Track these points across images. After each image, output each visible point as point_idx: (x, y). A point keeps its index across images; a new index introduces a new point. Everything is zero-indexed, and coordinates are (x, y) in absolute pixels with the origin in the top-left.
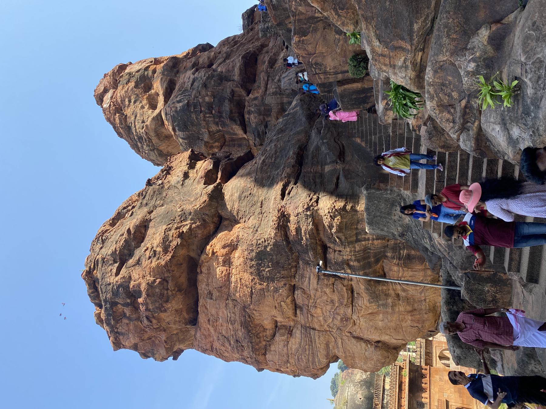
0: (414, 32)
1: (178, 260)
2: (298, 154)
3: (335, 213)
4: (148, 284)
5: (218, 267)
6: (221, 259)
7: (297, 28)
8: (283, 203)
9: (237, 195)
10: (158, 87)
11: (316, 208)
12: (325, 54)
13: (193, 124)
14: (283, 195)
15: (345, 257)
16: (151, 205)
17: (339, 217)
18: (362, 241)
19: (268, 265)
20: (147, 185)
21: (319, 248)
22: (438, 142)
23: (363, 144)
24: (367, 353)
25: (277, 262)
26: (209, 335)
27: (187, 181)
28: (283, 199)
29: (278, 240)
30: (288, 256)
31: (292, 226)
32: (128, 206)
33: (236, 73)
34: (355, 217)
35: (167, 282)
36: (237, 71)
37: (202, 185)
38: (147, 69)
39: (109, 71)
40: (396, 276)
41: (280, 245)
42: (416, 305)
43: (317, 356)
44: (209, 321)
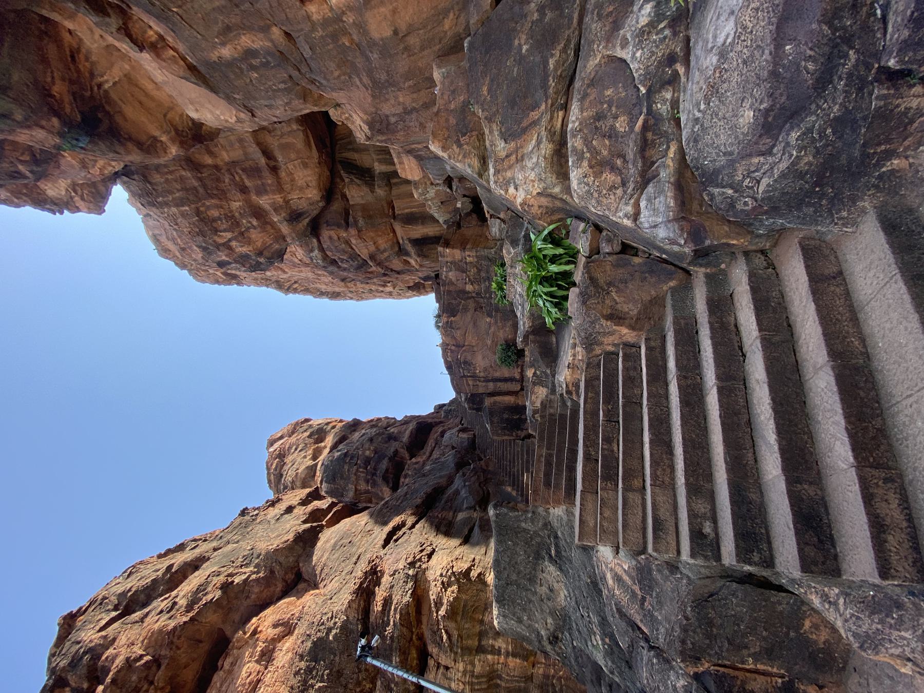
0: (549, 76)
1: (199, 630)
4: (128, 659)
5: (249, 662)
6: (261, 646)
8: (382, 552)
10: (329, 440)
11: (424, 566)
12: (475, 349)
13: (342, 478)
14: (387, 542)
17: (455, 588)
21: (414, 654)
23: (514, 493)
27: (286, 516)
28: (384, 547)
29: (351, 618)
35: (159, 666)
36: (408, 433)
38: (327, 424)
39: (294, 421)
41: (352, 631)
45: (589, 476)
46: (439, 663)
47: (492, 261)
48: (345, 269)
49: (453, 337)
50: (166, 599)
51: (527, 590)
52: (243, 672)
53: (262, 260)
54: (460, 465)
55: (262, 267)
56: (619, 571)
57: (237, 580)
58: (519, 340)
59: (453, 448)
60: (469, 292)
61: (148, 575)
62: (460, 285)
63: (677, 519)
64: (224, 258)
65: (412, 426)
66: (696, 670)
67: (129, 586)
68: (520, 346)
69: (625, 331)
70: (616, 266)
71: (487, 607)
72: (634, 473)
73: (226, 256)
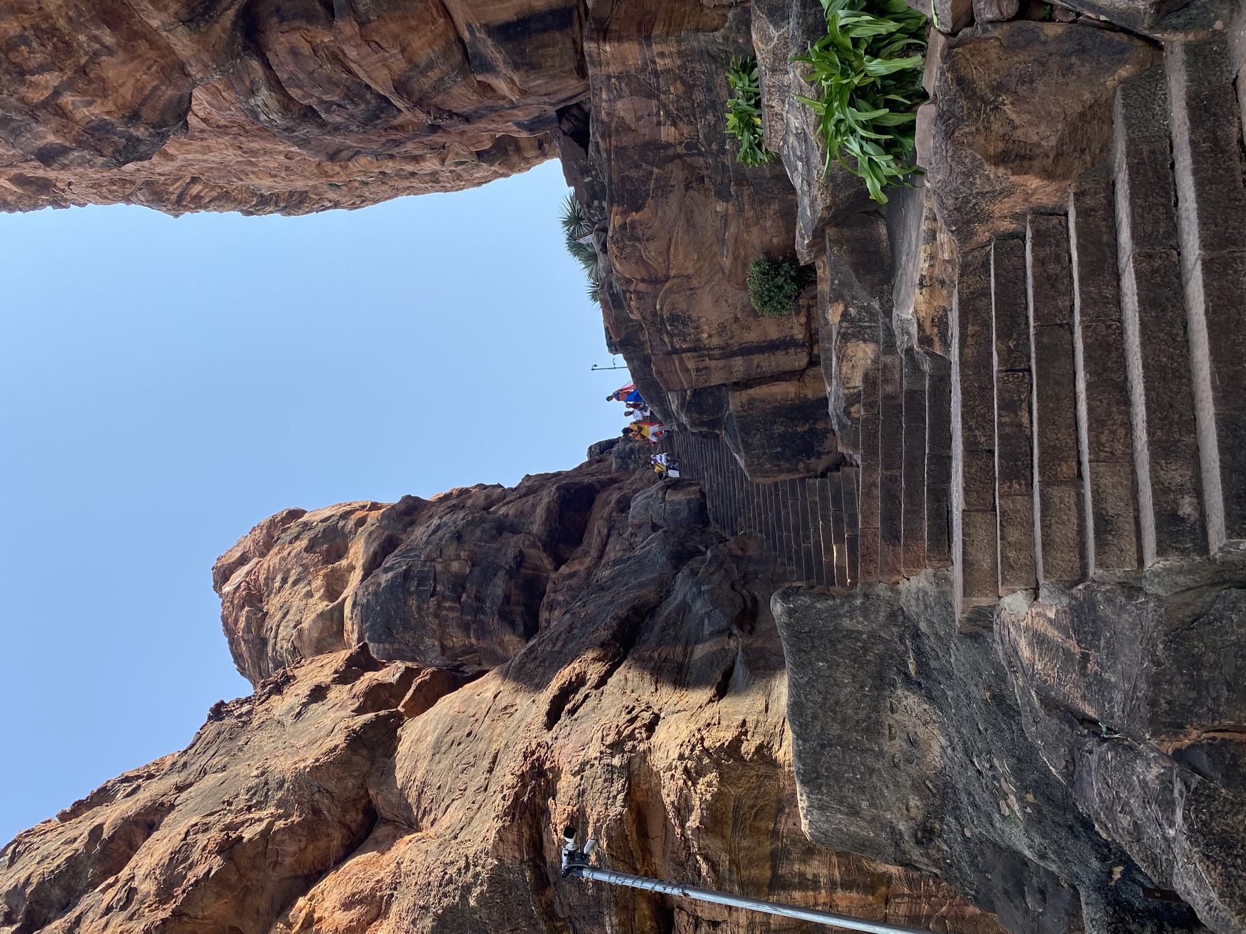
2: (627, 618)
3: (700, 759)
7: (615, 179)
8: (547, 737)
10: (358, 552)
11: (642, 747)
12: (695, 283)
13: (406, 626)
14: (553, 717)
16: (194, 767)
17: (712, 776)
18: (795, 888)
20: (210, 718)
27: (314, 706)
28: (549, 726)
29: (508, 861)
31: (560, 808)
36: (540, 512)
38: (345, 515)
39: (264, 519)
41: (513, 886)
45: (977, 485)
46: (697, 918)
47: (717, 59)
48: (336, 129)
49: (641, 261)
50: (110, 886)
51: (864, 751)
53: (140, 132)
54: (681, 557)
55: (142, 148)
56: (1041, 626)
58: (802, 243)
59: (655, 527)
60: (668, 145)
61: (55, 850)
62: (646, 131)
63: (1137, 510)
64: (51, 138)
65: (547, 496)
66: (1177, 745)
67: (23, 876)
68: (804, 258)
69: (1033, 182)
70: (1009, 47)
71: (785, 804)
72: (1060, 453)
73: (56, 132)
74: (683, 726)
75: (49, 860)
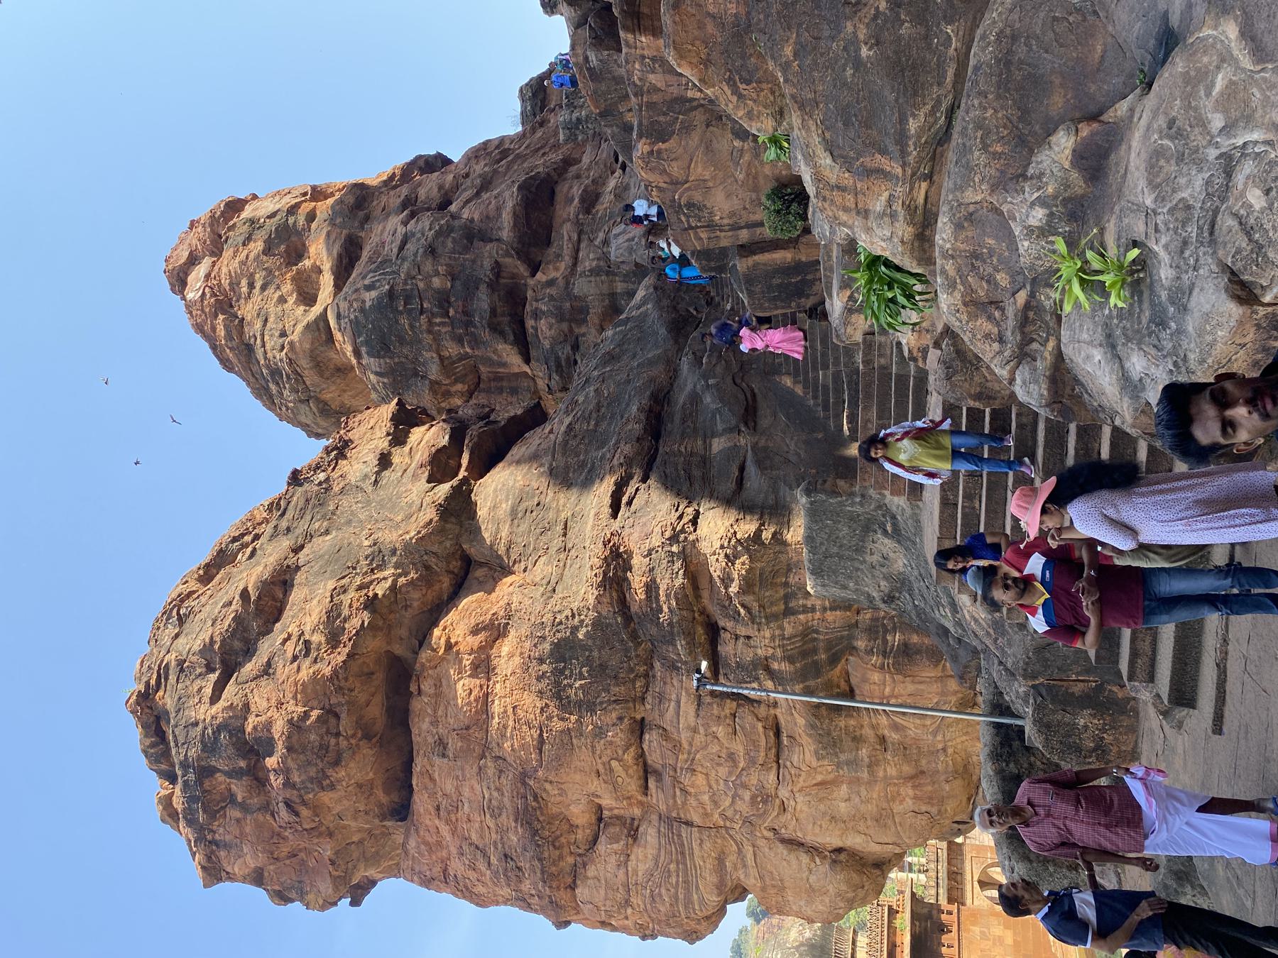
0: (908, 138)
2: (650, 411)
3: (735, 547)
4: (290, 722)
5: (459, 679)
6: (467, 661)
8: (615, 525)
9: (506, 507)
10: (320, 253)
11: (691, 538)
12: (711, 184)
13: (402, 341)
14: (615, 508)
15: (759, 652)
16: (298, 531)
19: (581, 673)
20: (289, 484)
21: (700, 630)
22: (966, 385)
23: (799, 390)
24: (813, 878)
25: (601, 665)
26: (439, 844)
27: (386, 473)
29: (604, 613)
30: (627, 650)
31: (637, 579)
32: (243, 535)
33: (506, 224)
34: (783, 557)
35: (337, 716)
36: (506, 218)
37: (423, 484)
38: (293, 210)
40: (877, 693)
41: (608, 625)
42: (924, 762)
43: (697, 888)
44: (438, 809)
52: (460, 691)
57: (380, 590)
74: (719, 523)
75: (219, 622)
